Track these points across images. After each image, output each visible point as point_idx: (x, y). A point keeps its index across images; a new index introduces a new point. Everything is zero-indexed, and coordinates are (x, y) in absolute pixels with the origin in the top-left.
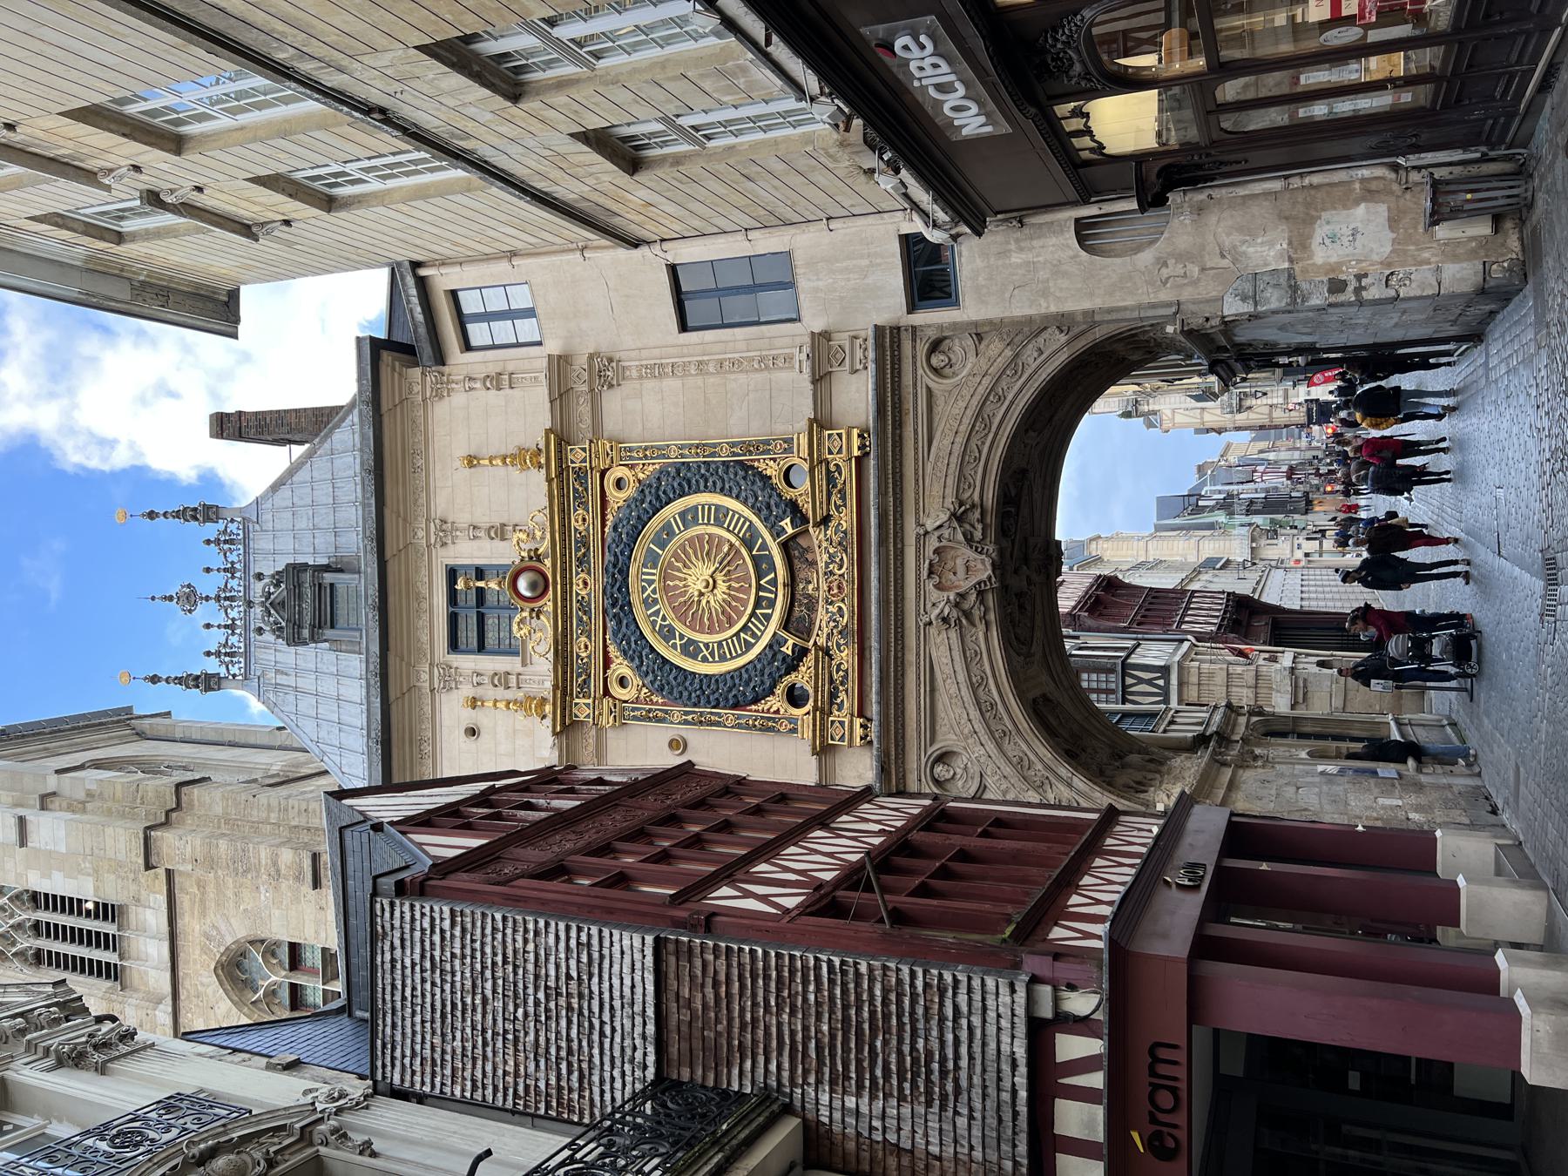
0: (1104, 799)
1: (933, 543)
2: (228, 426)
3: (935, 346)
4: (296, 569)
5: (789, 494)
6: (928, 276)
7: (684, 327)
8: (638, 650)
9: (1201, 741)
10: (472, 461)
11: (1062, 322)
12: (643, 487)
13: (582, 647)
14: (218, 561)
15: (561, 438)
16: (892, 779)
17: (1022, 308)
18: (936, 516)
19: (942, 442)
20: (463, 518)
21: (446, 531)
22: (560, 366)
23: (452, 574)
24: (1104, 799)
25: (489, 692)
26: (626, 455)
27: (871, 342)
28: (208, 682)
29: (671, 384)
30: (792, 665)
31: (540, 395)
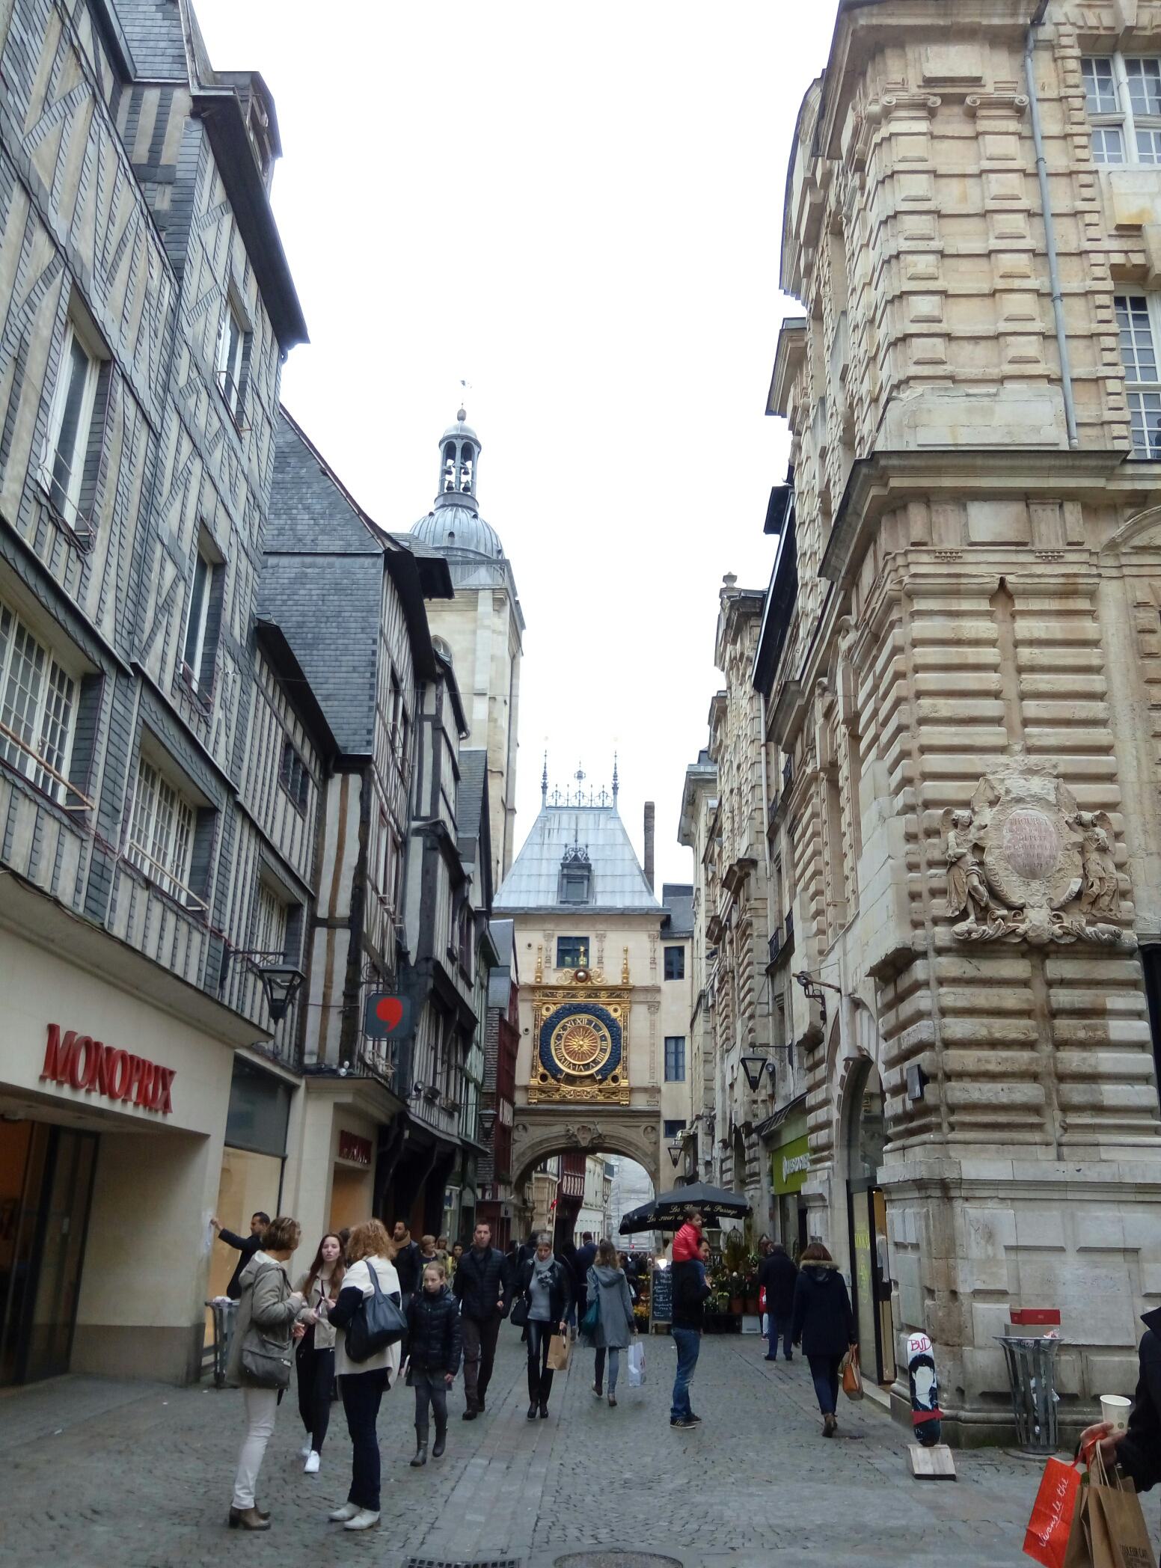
1: (592, 1127)
3: (653, 1128)
4: (588, 867)
5: (610, 1077)
6: (673, 1126)
7: (667, 1039)
8: (559, 1016)
9: (525, 1201)
12: (614, 1020)
15: (631, 990)
16: (517, 1112)
18: (601, 1129)
20: (607, 944)
21: (601, 938)
22: (657, 990)
23: (585, 940)
24: (514, 1179)
26: (625, 1017)
27: (656, 1108)
28: (544, 787)
29: (647, 1032)
30: (554, 1077)
31: (647, 982)
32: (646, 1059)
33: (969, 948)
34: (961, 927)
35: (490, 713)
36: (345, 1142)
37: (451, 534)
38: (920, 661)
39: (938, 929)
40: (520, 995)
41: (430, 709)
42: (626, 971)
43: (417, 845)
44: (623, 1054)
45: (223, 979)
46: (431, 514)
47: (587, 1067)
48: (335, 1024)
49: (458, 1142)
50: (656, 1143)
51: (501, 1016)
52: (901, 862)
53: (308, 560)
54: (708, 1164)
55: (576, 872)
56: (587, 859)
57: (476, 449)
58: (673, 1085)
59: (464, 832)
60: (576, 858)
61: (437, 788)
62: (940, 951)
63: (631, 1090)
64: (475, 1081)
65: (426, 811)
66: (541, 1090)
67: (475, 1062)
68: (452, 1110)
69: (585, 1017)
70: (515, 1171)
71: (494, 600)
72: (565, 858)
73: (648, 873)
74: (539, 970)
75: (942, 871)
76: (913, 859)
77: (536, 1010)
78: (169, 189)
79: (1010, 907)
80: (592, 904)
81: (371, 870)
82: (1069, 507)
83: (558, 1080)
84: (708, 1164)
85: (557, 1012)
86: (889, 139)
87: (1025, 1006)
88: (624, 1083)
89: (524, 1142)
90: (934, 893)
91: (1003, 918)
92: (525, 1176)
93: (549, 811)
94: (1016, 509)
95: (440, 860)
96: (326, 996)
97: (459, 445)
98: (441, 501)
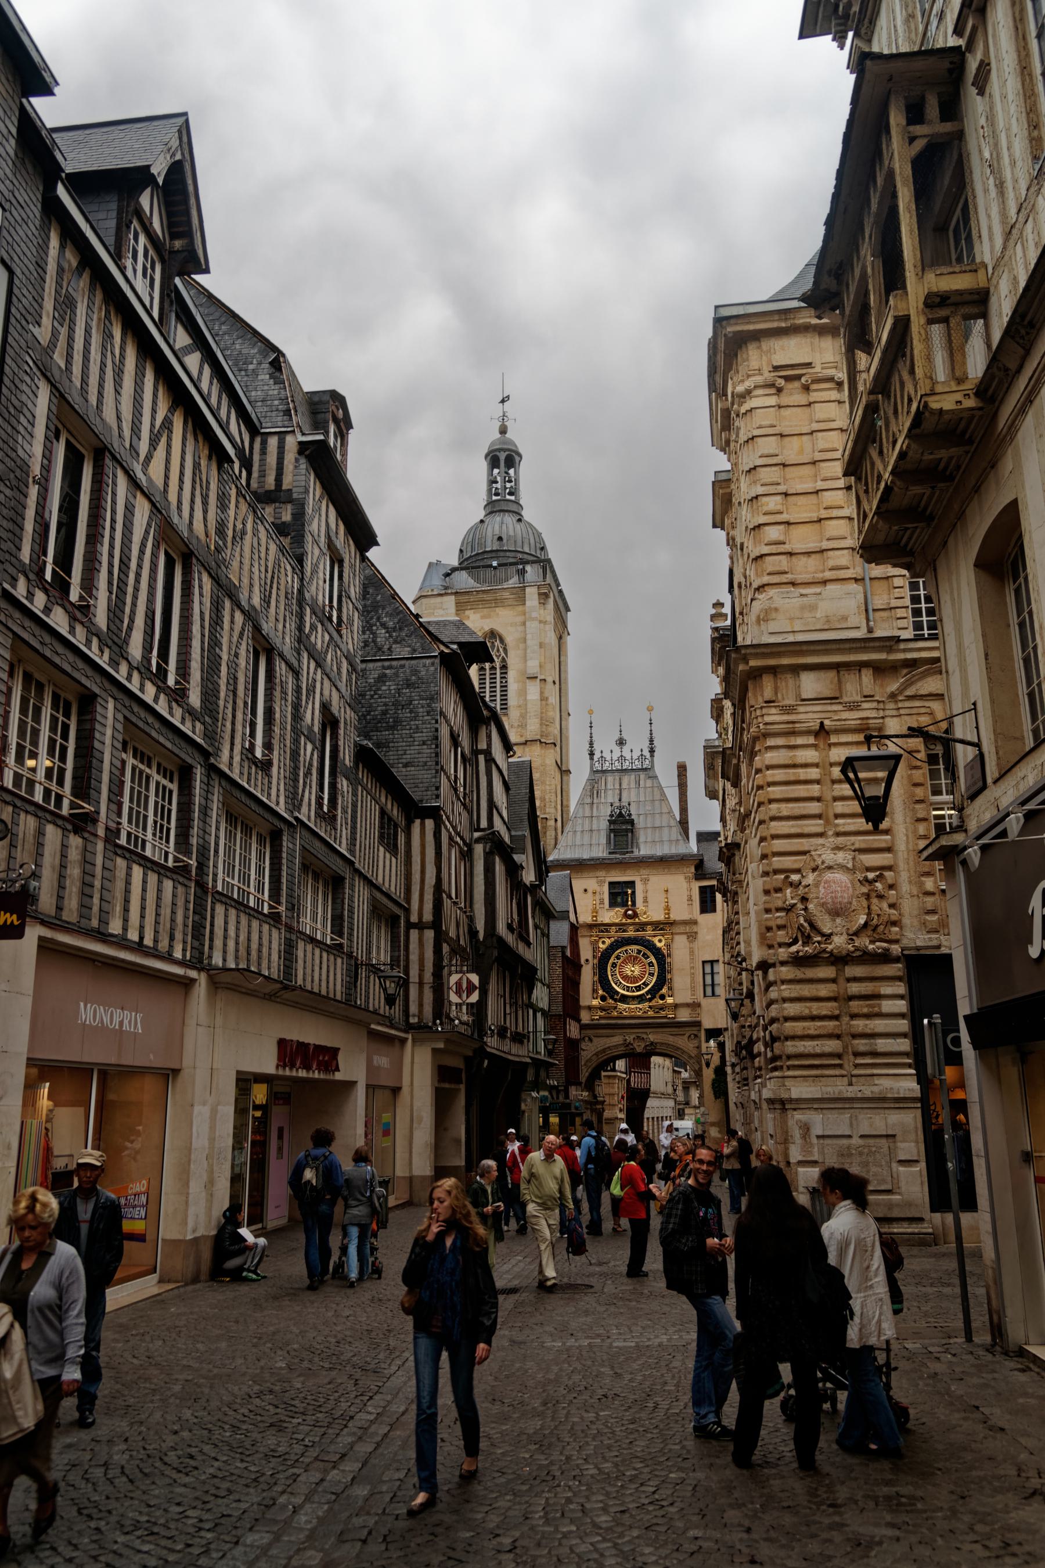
4: (632, 822)
7: (704, 962)
9: (595, 1097)
12: (659, 949)
14: (635, 757)
15: (672, 924)
16: (583, 1027)
18: (652, 1037)
20: (649, 886)
21: (645, 881)
22: (695, 922)
23: (633, 883)
25: (598, 897)
28: (592, 754)
29: (688, 957)
30: (612, 998)
31: (686, 917)
32: (688, 980)
33: (798, 961)
34: (794, 949)
35: (542, 693)
36: (444, 1074)
37: (500, 539)
38: (770, 779)
39: (781, 950)
40: (581, 932)
41: (482, 745)
42: (667, 908)
43: (479, 849)
44: (668, 976)
45: (356, 981)
46: (482, 521)
47: (638, 988)
48: (428, 996)
49: (528, 1060)
50: (699, 1047)
51: (563, 953)
52: (761, 907)
53: (387, 664)
54: (733, 1065)
55: (622, 827)
56: (630, 815)
57: (517, 458)
59: (515, 830)
61: (492, 805)
62: (783, 963)
63: (676, 1006)
64: (542, 1010)
65: (484, 824)
66: (602, 1009)
67: (540, 995)
68: (519, 1038)
69: (635, 947)
70: (584, 1075)
71: (540, 594)
72: (611, 816)
73: (684, 823)
74: (595, 911)
75: (783, 914)
76: (768, 906)
77: (594, 944)
78: (289, 507)
79: (823, 935)
80: (636, 853)
81: (445, 887)
82: (864, 671)
83: (615, 1000)
85: (611, 945)
86: (751, 410)
87: (831, 995)
89: (589, 1051)
90: (780, 927)
91: (819, 942)
92: (595, 1075)
93: (598, 774)
94: (832, 674)
95: (497, 859)
96: (421, 977)
97: (502, 456)
98: (489, 509)
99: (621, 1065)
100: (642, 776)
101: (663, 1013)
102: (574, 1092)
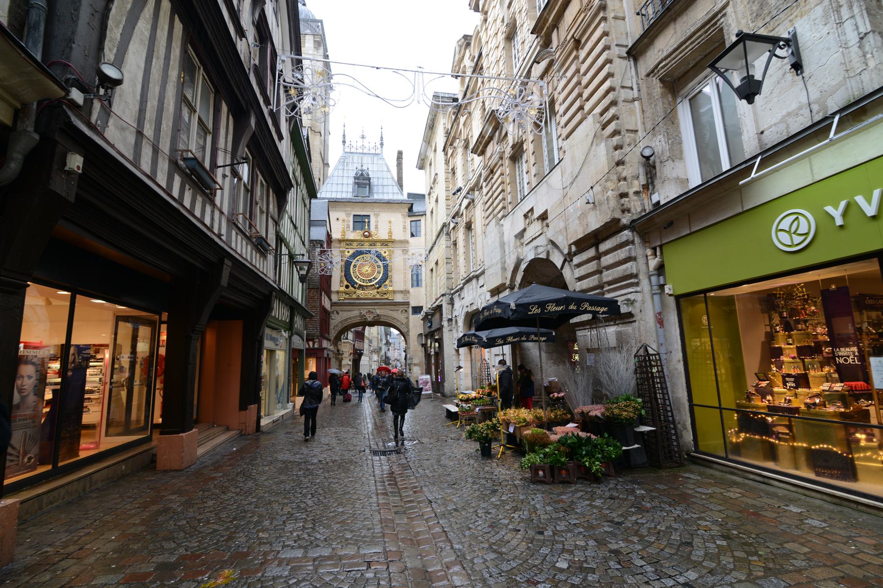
0: (332, 339)
2: (400, 153)
4: (369, 179)
6: (417, 310)
8: (354, 256)
9: (338, 351)
10: (390, 222)
11: (408, 331)
13: (355, 243)
16: (333, 304)
17: (411, 325)
18: (378, 312)
19: (391, 312)
20: (380, 219)
21: (377, 215)
24: (332, 339)
25: (346, 223)
28: (344, 142)
30: (353, 286)
31: (402, 238)
32: (402, 276)
42: (390, 233)
44: (390, 274)
47: (370, 281)
55: (363, 181)
58: (416, 289)
60: (362, 174)
63: (394, 292)
70: (333, 334)
84: (450, 320)
88: (391, 289)
89: (336, 321)
92: (338, 338)
93: (347, 155)
99: (350, 336)
100: (375, 159)
101: (385, 296)
102: (325, 344)
